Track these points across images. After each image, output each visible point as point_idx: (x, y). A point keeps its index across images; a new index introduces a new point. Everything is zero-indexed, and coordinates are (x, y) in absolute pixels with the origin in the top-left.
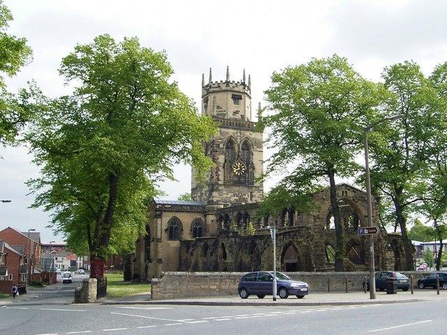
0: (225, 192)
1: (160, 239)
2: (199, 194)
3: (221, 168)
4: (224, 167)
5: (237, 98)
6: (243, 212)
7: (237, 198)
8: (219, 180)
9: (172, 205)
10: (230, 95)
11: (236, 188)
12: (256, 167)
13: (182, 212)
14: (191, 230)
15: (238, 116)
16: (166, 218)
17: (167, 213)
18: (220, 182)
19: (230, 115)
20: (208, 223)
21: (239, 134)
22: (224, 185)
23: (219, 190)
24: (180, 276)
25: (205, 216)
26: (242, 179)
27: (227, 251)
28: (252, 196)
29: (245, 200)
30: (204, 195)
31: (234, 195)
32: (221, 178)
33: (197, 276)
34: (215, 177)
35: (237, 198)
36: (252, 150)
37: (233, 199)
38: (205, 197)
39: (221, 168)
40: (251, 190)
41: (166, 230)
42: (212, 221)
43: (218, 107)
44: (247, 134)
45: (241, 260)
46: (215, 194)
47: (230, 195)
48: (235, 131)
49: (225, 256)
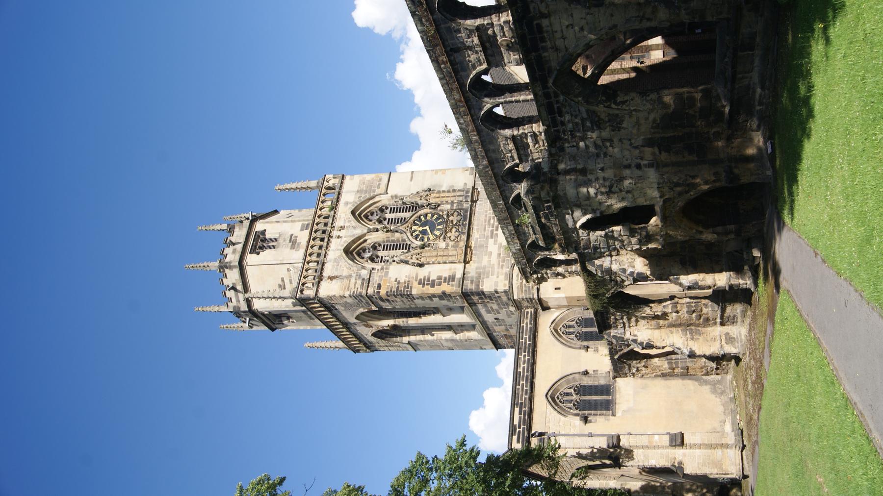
0: (485, 261)
1: (610, 437)
3: (423, 273)
4: (421, 265)
8: (452, 278)
9: (514, 405)
12: (426, 187)
13: (533, 375)
15: (303, 237)
16: (546, 418)
17: (536, 416)
18: (459, 275)
19: (298, 255)
21: (342, 233)
22: (466, 262)
23: (479, 277)
30: (500, 316)
34: (446, 288)
36: (385, 200)
39: (423, 273)
41: (586, 420)
43: (282, 287)
44: (344, 213)
45: (649, 143)
46: (487, 287)
48: (334, 241)
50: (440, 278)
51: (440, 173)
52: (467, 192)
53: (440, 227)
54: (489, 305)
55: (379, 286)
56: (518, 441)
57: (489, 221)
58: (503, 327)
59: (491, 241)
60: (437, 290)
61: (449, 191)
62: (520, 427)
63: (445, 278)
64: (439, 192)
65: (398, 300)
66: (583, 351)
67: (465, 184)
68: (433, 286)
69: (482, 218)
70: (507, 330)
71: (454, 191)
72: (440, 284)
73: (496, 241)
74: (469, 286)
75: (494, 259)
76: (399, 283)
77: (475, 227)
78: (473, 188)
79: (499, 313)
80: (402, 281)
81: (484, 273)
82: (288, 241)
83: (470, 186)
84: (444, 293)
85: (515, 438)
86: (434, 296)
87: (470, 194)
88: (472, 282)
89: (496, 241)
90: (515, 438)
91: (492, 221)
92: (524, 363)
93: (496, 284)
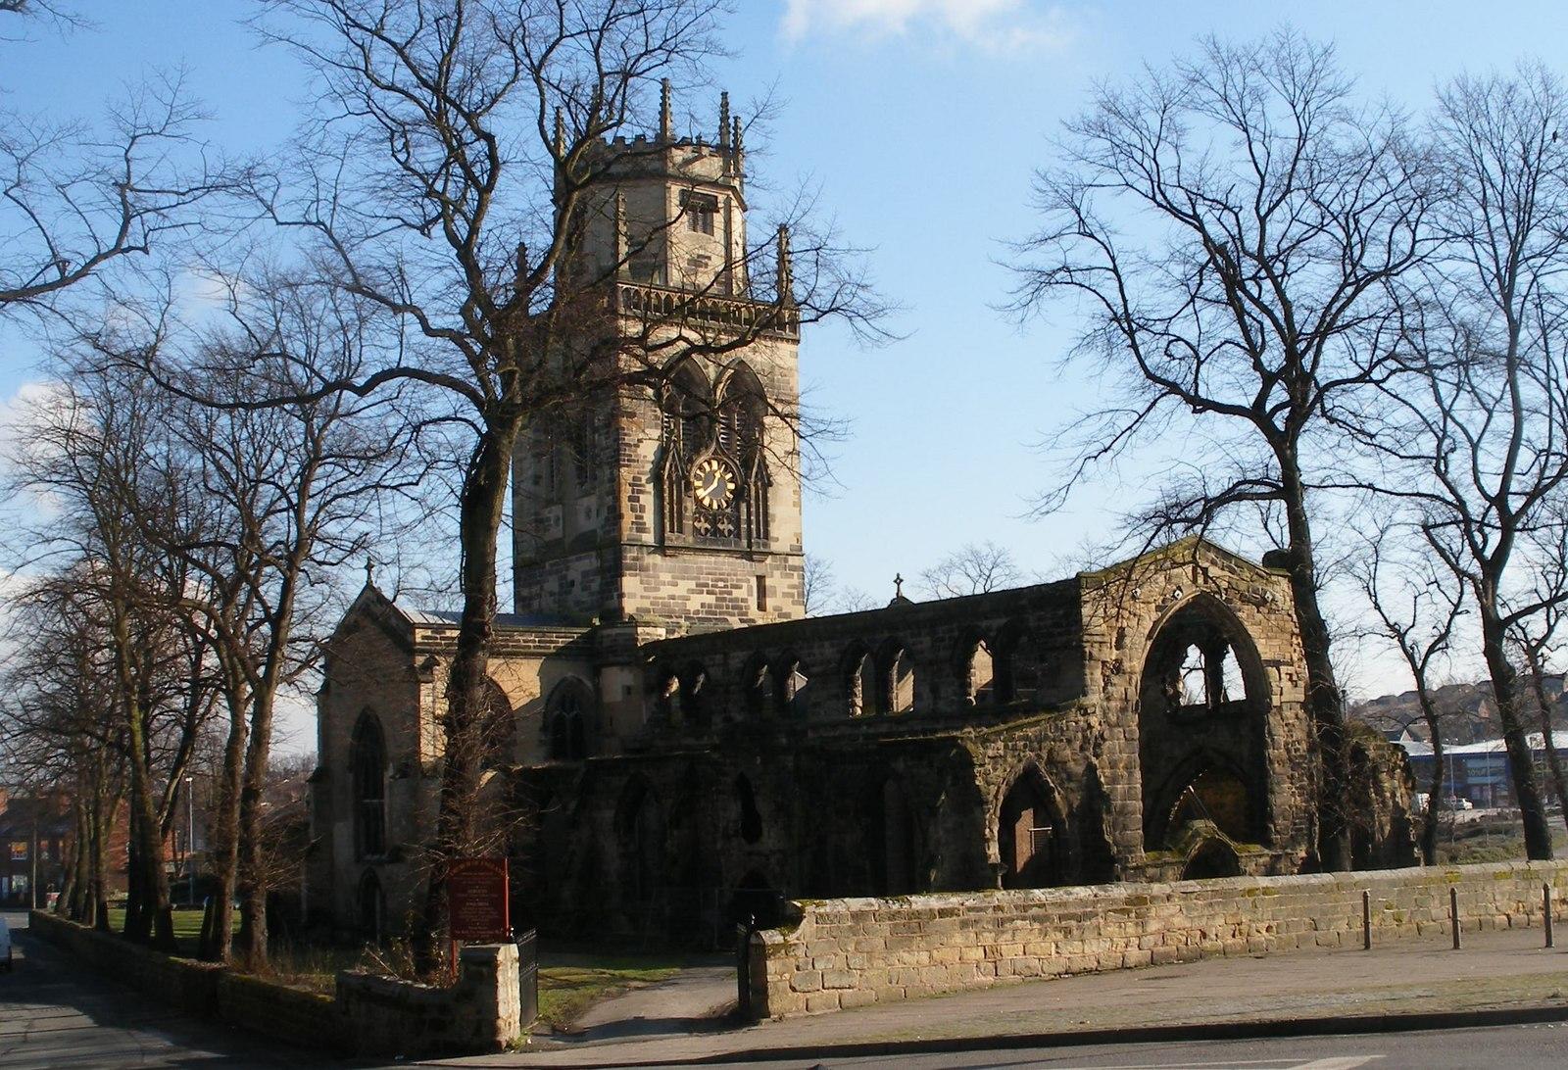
0: (666, 577)
2: (552, 584)
5: (701, 210)
6: (772, 653)
7: (710, 599)
10: (675, 190)
11: (706, 561)
14: (544, 729)
20: (607, 699)
24: (857, 916)
25: (596, 673)
26: (725, 527)
27: (763, 807)
28: (762, 592)
29: (738, 607)
31: (701, 587)
32: (649, 518)
33: (918, 914)
35: (710, 599)
37: (694, 604)
38: (585, 597)
40: (760, 569)
42: (628, 690)
46: (630, 583)
47: (685, 586)
49: (751, 828)
50: (642, 509)
51: (795, 498)
52: (765, 545)
53: (715, 506)
54: (598, 580)
55: (632, 415)
56: (424, 637)
57: (721, 580)
58: (556, 589)
59: (692, 584)
60: (625, 505)
61: (766, 514)
62: (441, 638)
63: (642, 518)
64: (765, 499)
65: (610, 441)
66: (540, 724)
67: (777, 540)
68: (631, 499)
69: (726, 569)
70: (552, 594)
71: (766, 524)
72: (633, 509)
73: (692, 591)
74: (630, 555)
75: (665, 591)
76: (637, 446)
77: (713, 559)
78: (772, 553)
79: (583, 590)
80: (639, 451)
81: (648, 576)
82: (701, 252)
83: (774, 547)
84: (620, 516)
85: (429, 633)
86: (617, 499)
87: (762, 549)
88: (636, 559)
89: (692, 591)
90: (429, 633)
91: (721, 584)
92: (525, 641)
93: (633, 596)
